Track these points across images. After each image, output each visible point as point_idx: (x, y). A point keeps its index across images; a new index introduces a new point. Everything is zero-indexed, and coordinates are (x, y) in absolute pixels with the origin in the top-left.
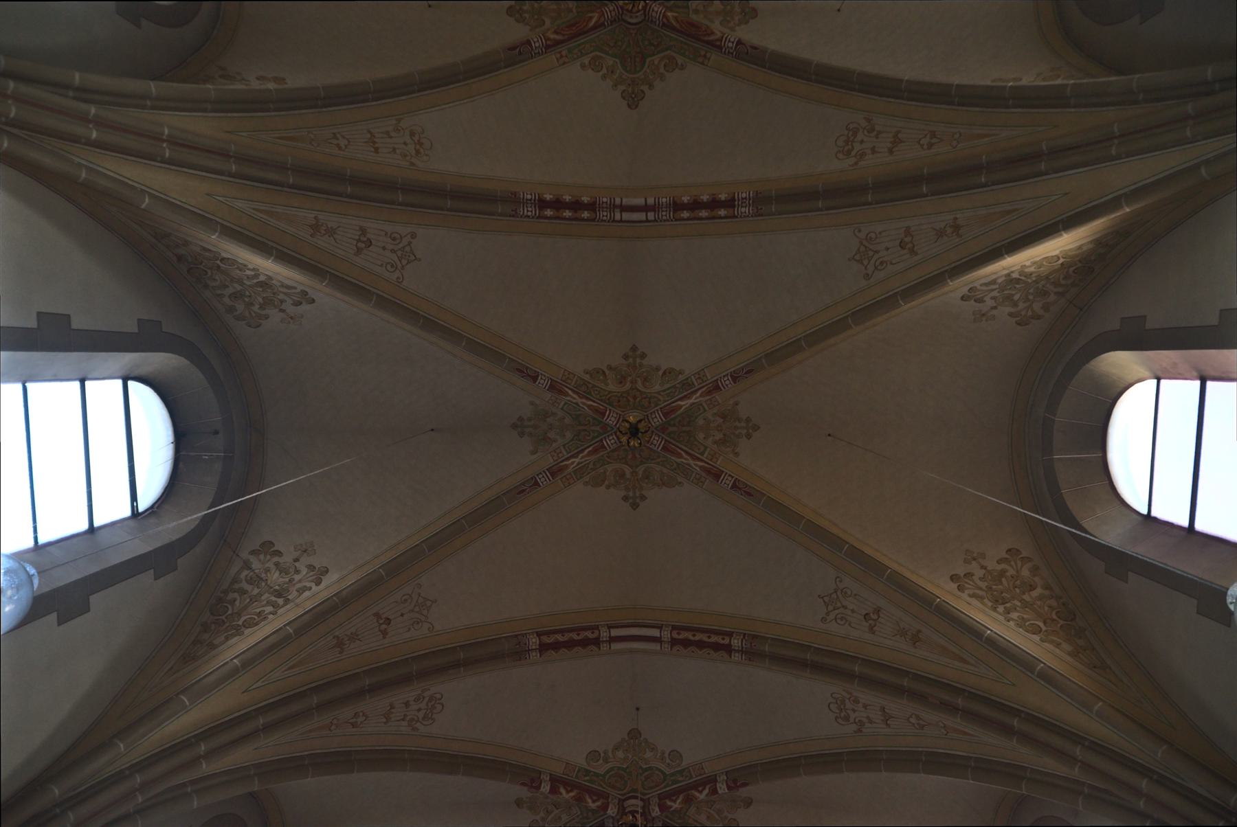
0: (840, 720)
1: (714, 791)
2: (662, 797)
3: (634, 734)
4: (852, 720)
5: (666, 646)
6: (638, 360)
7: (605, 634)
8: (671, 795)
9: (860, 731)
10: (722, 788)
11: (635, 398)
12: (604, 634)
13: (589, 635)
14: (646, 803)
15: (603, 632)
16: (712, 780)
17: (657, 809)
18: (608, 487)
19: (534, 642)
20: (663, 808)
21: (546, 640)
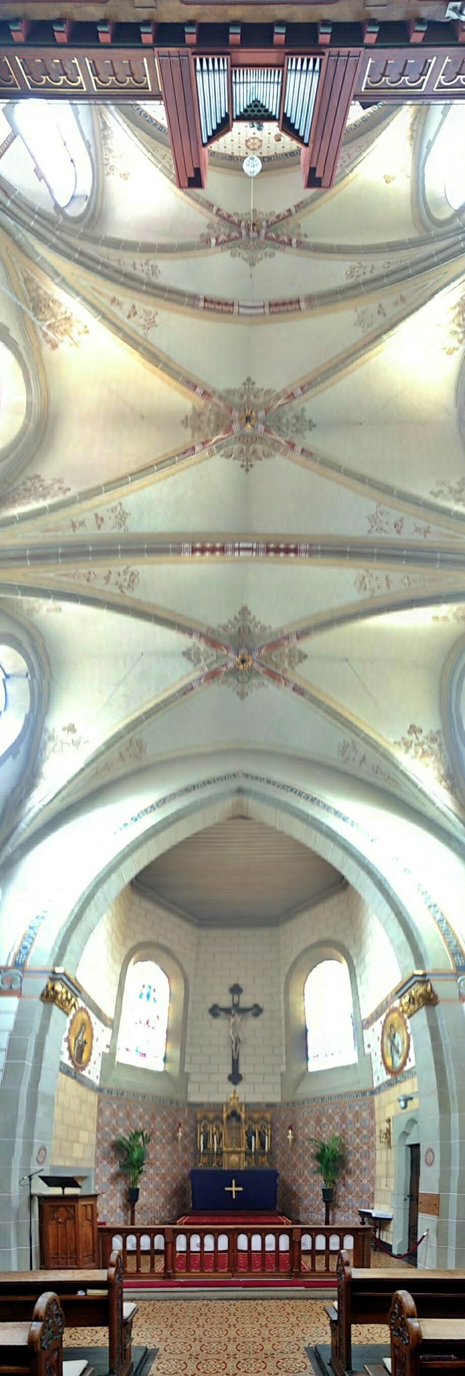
1: (217, 239)
8: (236, 238)
10: (213, 241)
14: (248, 235)
18: (262, 389)
20: (240, 233)
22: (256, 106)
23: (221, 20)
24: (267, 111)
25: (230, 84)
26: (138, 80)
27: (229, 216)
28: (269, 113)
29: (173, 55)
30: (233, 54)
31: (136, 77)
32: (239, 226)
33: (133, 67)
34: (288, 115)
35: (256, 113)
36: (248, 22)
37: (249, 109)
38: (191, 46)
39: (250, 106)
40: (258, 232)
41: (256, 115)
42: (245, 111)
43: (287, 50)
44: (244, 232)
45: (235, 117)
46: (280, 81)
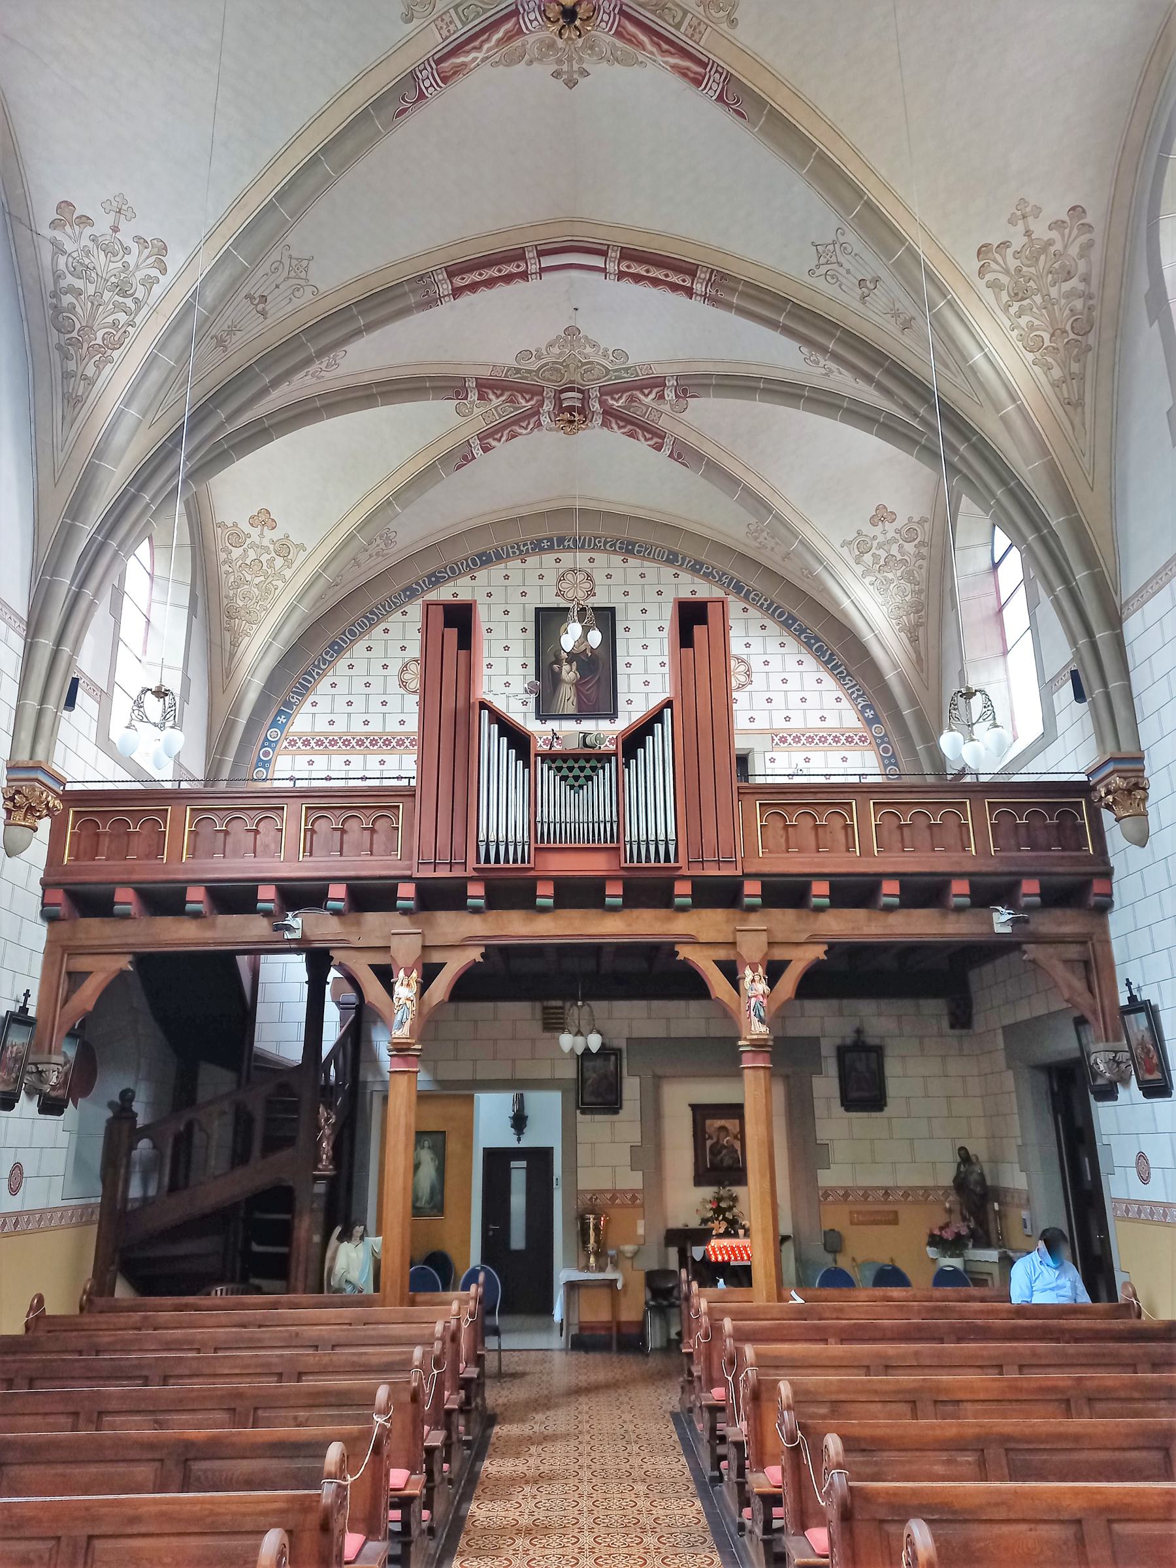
0: (808, 361)
2: (603, 391)
3: (572, 331)
4: (821, 364)
5: (612, 277)
7: (534, 266)
9: (826, 374)
12: (533, 268)
13: (511, 269)
14: (585, 399)
15: (532, 264)
17: (597, 405)
18: (531, 62)
19: (446, 288)
21: (458, 282)
23: (636, 912)
26: (777, 818)
27: (631, 435)
29: (713, 863)
31: (780, 824)
32: (605, 413)
33: (783, 840)
36: (594, 911)
38: (684, 878)
40: (558, 401)
44: (596, 406)
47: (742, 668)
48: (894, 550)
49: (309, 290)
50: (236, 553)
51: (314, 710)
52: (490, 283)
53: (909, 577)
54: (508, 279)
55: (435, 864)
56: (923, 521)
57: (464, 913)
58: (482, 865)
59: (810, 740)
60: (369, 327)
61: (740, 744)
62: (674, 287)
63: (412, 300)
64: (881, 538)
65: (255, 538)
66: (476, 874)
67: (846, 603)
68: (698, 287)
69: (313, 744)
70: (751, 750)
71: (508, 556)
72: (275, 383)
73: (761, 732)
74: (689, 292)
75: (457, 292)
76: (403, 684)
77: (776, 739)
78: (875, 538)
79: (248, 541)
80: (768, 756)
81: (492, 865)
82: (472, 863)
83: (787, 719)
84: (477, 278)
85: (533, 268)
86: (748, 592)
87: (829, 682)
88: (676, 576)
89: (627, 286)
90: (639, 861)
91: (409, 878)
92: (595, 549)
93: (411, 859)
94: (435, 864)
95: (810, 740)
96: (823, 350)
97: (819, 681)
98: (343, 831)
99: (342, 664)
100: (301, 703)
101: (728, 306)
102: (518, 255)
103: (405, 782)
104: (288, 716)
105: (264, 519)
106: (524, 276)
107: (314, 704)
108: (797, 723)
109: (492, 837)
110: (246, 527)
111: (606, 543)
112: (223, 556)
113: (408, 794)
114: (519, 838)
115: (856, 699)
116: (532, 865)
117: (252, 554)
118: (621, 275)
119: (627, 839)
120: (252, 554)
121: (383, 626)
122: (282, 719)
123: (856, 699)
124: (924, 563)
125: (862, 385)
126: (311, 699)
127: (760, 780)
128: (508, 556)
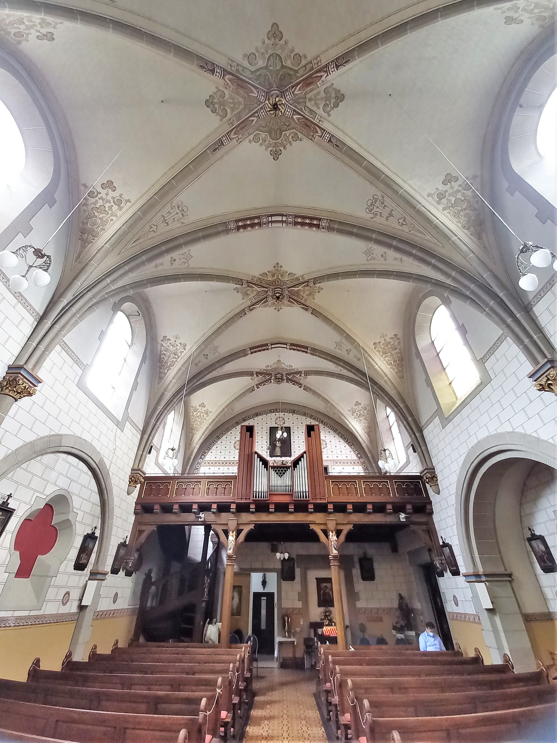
6: (279, 268)
11: (278, 282)
12: (270, 347)
14: (282, 375)
16: (301, 372)
19: (249, 352)
21: (252, 351)
22: (280, 473)
24: (276, 471)
25: (292, 486)
28: (274, 470)
30: (292, 500)
34: (265, 469)
35: (280, 470)
37: (284, 472)
39: (284, 473)
41: (280, 469)
42: (285, 471)
43: (268, 501)
45: (290, 468)
46: (270, 487)
47: (324, 443)
48: (361, 412)
49: (218, 353)
50: (195, 413)
51: (211, 454)
52: (260, 351)
53: (366, 419)
54: (264, 350)
55: (241, 498)
56: (368, 405)
57: (249, 513)
58: (255, 499)
59: (344, 463)
60: (231, 361)
61: (325, 464)
62: (303, 351)
63: (241, 355)
64: (358, 409)
65: (200, 410)
66: (252, 501)
67: (350, 426)
68: (308, 351)
69: (210, 463)
70: (328, 465)
71: (263, 414)
72: (208, 374)
73: (330, 460)
74: (307, 352)
75: (252, 353)
76: (235, 447)
77: (335, 463)
78: (356, 409)
79: (198, 410)
80: (333, 467)
81: (257, 499)
82: (252, 498)
83: (337, 457)
84: (257, 350)
85: (270, 347)
86: (325, 423)
87: (348, 447)
88: (306, 419)
89: (292, 351)
90: (298, 498)
91: (234, 503)
92: (285, 412)
93: (235, 496)
94: (241, 498)
95: (344, 463)
96: (340, 365)
97: (345, 446)
98: (217, 488)
99: (219, 442)
100: (208, 452)
101: (316, 356)
102: (267, 345)
103: (234, 474)
104: (204, 456)
105: (203, 405)
106: (268, 349)
107: (211, 452)
108: (340, 458)
109: (257, 490)
110: (198, 407)
111: (288, 410)
112: (192, 414)
113: (235, 478)
114: (265, 491)
115: (355, 451)
116: (268, 499)
117: (199, 414)
118: (290, 349)
119: (295, 491)
120: (199, 414)
121: (230, 432)
122: (203, 457)
123: (355, 451)
124: (369, 415)
125: (349, 373)
126: (211, 451)
127: (331, 474)
128: (263, 414)
